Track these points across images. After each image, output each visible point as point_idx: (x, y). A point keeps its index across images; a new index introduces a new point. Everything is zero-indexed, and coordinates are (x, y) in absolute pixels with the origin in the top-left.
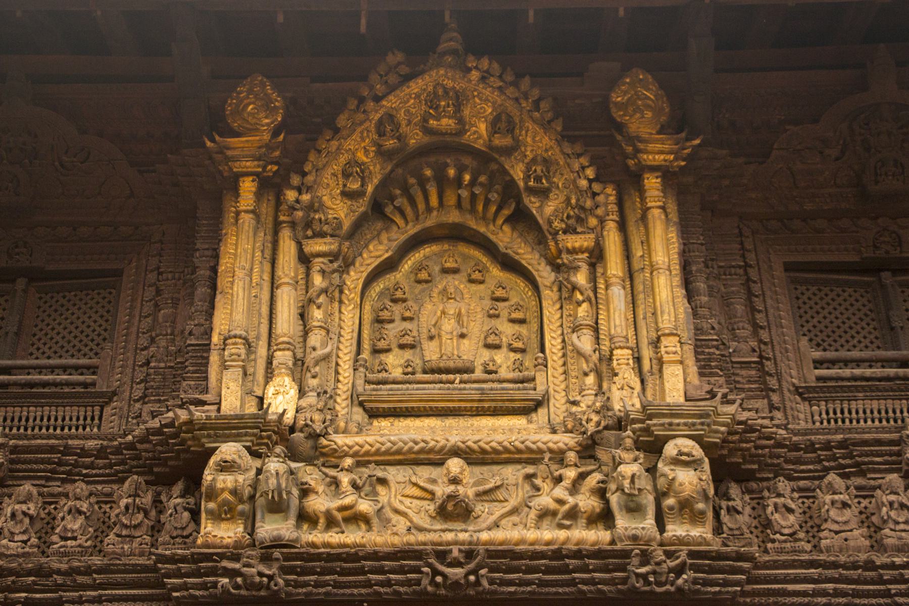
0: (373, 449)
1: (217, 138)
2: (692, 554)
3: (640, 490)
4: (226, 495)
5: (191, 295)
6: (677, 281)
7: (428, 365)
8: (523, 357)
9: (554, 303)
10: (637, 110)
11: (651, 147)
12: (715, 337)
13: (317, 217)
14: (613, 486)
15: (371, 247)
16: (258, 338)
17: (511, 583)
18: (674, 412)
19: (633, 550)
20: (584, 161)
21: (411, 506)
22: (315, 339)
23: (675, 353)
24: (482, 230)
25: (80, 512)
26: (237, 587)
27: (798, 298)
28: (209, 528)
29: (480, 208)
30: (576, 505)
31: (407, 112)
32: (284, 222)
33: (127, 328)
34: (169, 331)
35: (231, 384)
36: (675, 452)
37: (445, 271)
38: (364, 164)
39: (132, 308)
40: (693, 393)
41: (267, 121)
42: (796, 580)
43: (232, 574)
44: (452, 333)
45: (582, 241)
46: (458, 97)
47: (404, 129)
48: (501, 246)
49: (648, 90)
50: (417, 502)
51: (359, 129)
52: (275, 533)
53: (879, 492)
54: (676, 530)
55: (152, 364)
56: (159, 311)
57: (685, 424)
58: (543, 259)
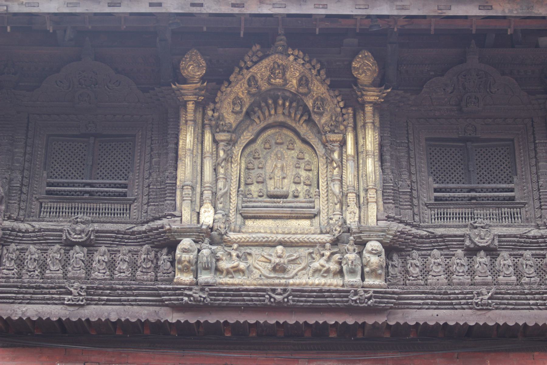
0: (246, 240)
1: (177, 85)
2: (375, 292)
3: (355, 265)
4: (186, 263)
5: (167, 153)
6: (377, 158)
7: (269, 193)
8: (310, 188)
9: (324, 165)
10: (364, 72)
11: (369, 93)
12: (392, 185)
13: (221, 123)
14: (344, 262)
15: (245, 134)
16: (196, 183)
17: (302, 301)
18: (371, 230)
19: (351, 290)
20: (339, 99)
22: (220, 184)
23: (374, 198)
24: (294, 125)
26: (191, 301)
27: (430, 154)
28: (179, 276)
29: (293, 115)
32: (207, 124)
33: (139, 166)
34: (157, 171)
35: (186, 208)
36: (370, 249)
37: (277, 143)
38: (242, 98)
39: (140, 156)
40: (380, 217)
41: (199, 73)
42: (417, 299)
43: (189, 296)
44: (279, 177)
45: (337, 137)
46: (284, 69)
47: (260, 82)
48: (302, 133)
49: (369, 61)
50: (264, 263)
51: (240, 82)
52: (206, 280)
53: (454, 257)
54: (369, 281)
55: (151, 187)
56: (153, 159)
57: (376, 235)
58: (320, 142)
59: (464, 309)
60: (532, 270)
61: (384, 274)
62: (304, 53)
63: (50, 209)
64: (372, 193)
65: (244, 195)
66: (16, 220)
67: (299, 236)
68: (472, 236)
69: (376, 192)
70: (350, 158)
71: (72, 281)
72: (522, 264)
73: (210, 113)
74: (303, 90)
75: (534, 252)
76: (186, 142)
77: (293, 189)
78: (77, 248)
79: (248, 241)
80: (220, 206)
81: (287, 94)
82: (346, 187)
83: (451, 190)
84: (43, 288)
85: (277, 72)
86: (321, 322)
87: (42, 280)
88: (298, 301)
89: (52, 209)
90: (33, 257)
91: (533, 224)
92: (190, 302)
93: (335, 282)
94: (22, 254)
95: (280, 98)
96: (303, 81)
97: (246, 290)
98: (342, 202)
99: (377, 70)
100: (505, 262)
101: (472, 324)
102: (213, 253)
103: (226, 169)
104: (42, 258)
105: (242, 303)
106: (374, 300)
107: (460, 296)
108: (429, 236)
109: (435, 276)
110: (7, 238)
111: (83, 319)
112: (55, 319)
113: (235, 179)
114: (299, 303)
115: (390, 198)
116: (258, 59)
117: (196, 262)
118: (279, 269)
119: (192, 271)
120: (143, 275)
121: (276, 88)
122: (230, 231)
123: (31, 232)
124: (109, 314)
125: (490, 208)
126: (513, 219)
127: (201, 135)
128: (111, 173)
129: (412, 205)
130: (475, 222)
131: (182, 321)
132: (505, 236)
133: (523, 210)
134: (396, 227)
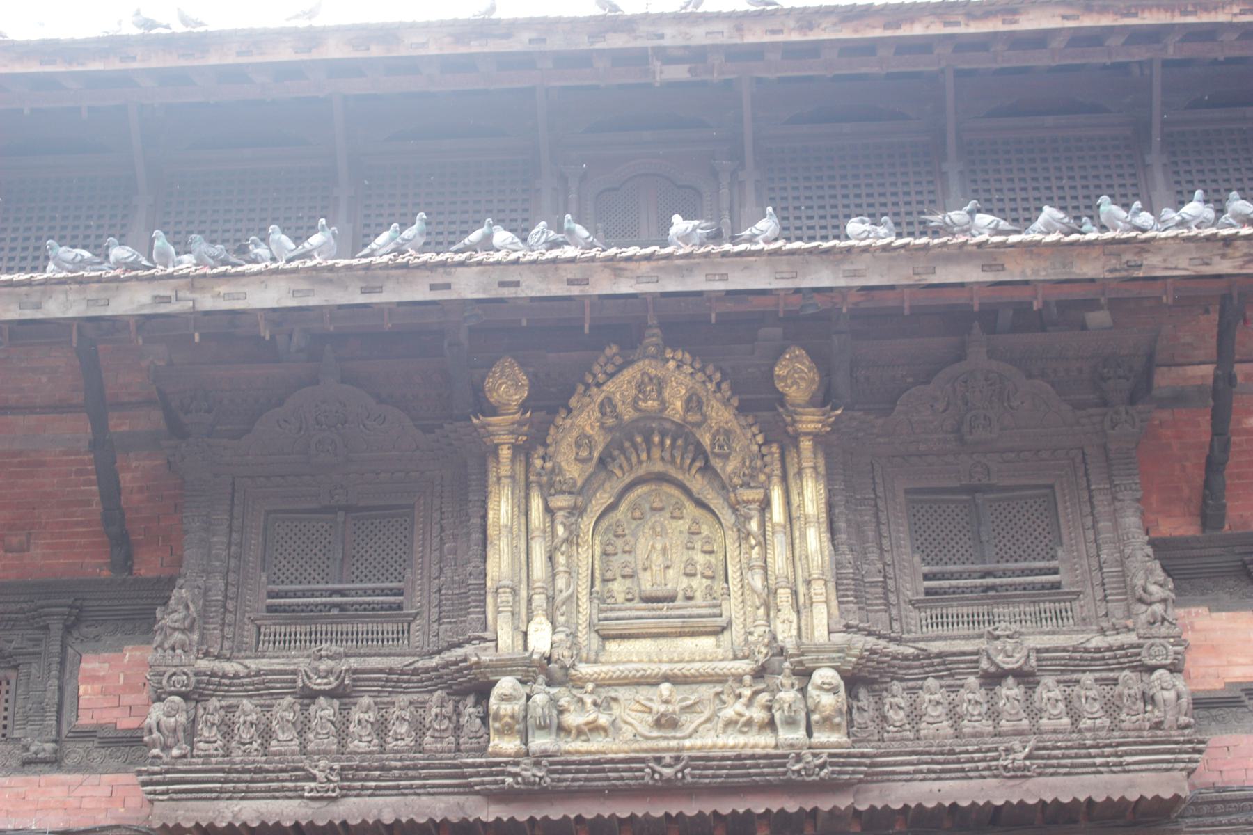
1: (481, 418)
2: (831, 755)
4: (507, 719)
5: (469, 534)
6: (824, 527)
7: (643, 595)
9: (734, 542)
10: (795, 382)
11: (804, 418)
14: (776, 706)
15: (598, 495)
16: (520, 582)
17: (707, 777)
19: (789, 754)
20: (755, 429)
21: (633, 717)
22: (561, 582)
24: (680, 477)
25: (404, 719)
26: (518, 783)
27: (914, 515)
29: (678, 461)
31: (622, 394)
33: (422, 557)
35: (504, 626)
36: (819, 682)
37: (653, 509)
38: (590, 436)
39: (424, 539)
40: (833, 627)
41: (517, 397)
43: (514, 775)
45: (756, 494)
46: (660, 384)
47: (620, 408)
49: (803, 364)
50: (639, 714)
52: (543, 747)
53: (962, 690)
55: (443, 592)
57: (828, 659)
58: (726, 504)
59: (984, 777)
60: (1097, 706)
61: (844, 724)
62: (693, 355)
63: (275, 636)
64: (818, 587)
65: (601, 599)
66: (217, 657)
67: (697, 665)
68: (992, 652)
69: (825, 585)
70: (778, 528)
71: (316, 757)
72: (1079, 697)
73: (538, 463)
74: (693, 418)
75: (1098, 675)
76: (499, 514)
77: (684, 586)
78: (322, 700)
79: (611, 678)
80: (561, 619)
81: (668, 425)
82: (773, 578)
83: (952, 576)
84: (268, 771)
85: (648, 388)
86: (741, 811)
87: (264, 758)
88: (701, 776)
89: (277, 637)
90: (249, 718)
91: (1095, 627)
92: (516, 786)
93: (762, 741)
94: (230, 715)
95: (656, 432)
96: (694, 403)
97: (612, 761)
98: (769, 604)
99: (817, 379)
100: (1051, 694)
101: (999, 802)
102: (553, 701)
103: (569, 557)
104: (264, 720)
105: (605, 783)
106: (830, 769)
107: (976, 756)
108: (918, 655)
109: (932, 724)
110: (204, 689)
111: (337, 822)
112: (288, 824)
113: (584, 573)
114: (703, 781)
115: (849, 593)
116: (615, 369)
117: (525, 717)
118: (666, 723)
119: (519, 732)
120: (436, 742)
121: (648, 416)
122: (580, 661)
123: (243, 677)
124: (380, 811)
125: (1019, 602)
126: (1060, 621)
127: (524, 501)
128: (375, 571)
129: (888, 604)
130: (996, 629)
131: (505, 819)
132: (1047, 650)
133: (1076, 605)
134: (861, 642)
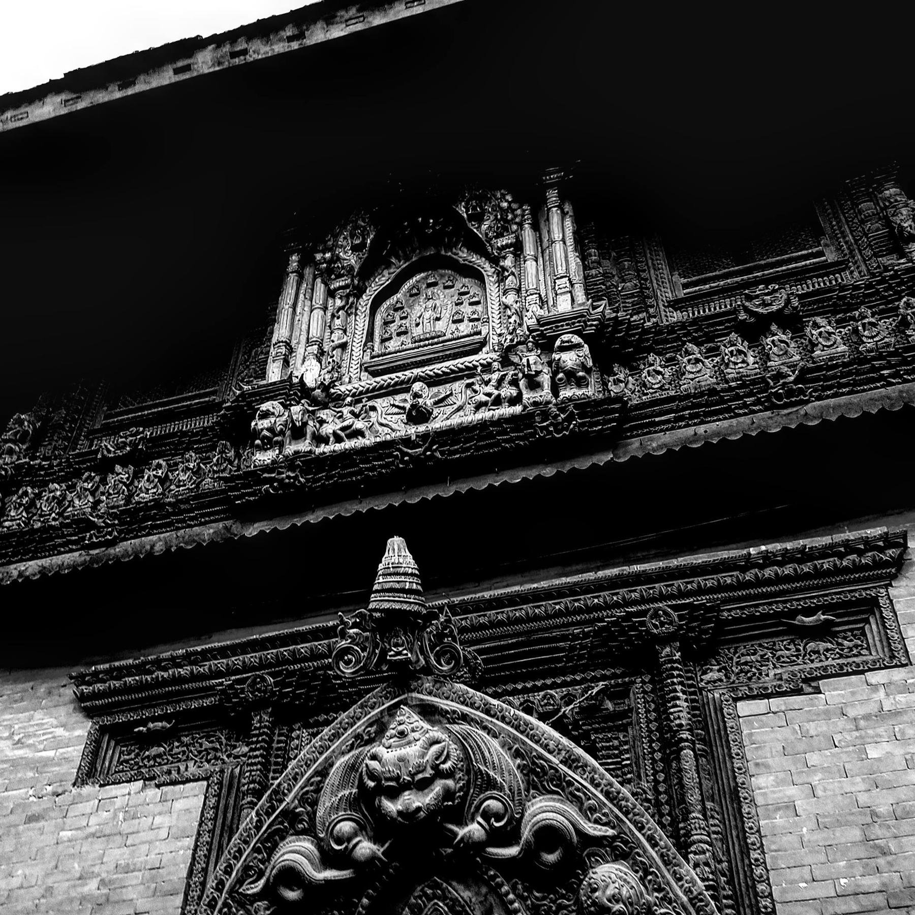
4: (265, 433)
19: (535, 412)
30: (499, 395)
37: (429, 285)
43: (270, 481)
54: (566, 393)
